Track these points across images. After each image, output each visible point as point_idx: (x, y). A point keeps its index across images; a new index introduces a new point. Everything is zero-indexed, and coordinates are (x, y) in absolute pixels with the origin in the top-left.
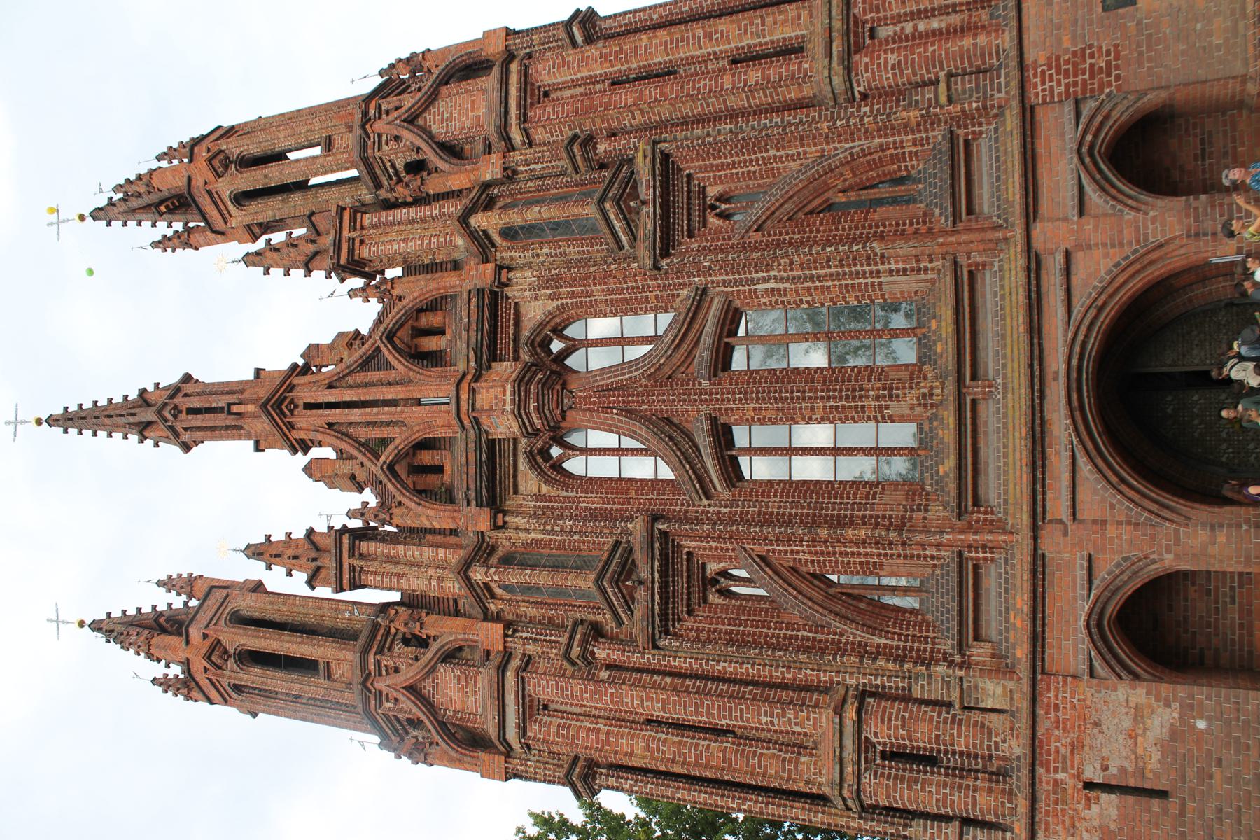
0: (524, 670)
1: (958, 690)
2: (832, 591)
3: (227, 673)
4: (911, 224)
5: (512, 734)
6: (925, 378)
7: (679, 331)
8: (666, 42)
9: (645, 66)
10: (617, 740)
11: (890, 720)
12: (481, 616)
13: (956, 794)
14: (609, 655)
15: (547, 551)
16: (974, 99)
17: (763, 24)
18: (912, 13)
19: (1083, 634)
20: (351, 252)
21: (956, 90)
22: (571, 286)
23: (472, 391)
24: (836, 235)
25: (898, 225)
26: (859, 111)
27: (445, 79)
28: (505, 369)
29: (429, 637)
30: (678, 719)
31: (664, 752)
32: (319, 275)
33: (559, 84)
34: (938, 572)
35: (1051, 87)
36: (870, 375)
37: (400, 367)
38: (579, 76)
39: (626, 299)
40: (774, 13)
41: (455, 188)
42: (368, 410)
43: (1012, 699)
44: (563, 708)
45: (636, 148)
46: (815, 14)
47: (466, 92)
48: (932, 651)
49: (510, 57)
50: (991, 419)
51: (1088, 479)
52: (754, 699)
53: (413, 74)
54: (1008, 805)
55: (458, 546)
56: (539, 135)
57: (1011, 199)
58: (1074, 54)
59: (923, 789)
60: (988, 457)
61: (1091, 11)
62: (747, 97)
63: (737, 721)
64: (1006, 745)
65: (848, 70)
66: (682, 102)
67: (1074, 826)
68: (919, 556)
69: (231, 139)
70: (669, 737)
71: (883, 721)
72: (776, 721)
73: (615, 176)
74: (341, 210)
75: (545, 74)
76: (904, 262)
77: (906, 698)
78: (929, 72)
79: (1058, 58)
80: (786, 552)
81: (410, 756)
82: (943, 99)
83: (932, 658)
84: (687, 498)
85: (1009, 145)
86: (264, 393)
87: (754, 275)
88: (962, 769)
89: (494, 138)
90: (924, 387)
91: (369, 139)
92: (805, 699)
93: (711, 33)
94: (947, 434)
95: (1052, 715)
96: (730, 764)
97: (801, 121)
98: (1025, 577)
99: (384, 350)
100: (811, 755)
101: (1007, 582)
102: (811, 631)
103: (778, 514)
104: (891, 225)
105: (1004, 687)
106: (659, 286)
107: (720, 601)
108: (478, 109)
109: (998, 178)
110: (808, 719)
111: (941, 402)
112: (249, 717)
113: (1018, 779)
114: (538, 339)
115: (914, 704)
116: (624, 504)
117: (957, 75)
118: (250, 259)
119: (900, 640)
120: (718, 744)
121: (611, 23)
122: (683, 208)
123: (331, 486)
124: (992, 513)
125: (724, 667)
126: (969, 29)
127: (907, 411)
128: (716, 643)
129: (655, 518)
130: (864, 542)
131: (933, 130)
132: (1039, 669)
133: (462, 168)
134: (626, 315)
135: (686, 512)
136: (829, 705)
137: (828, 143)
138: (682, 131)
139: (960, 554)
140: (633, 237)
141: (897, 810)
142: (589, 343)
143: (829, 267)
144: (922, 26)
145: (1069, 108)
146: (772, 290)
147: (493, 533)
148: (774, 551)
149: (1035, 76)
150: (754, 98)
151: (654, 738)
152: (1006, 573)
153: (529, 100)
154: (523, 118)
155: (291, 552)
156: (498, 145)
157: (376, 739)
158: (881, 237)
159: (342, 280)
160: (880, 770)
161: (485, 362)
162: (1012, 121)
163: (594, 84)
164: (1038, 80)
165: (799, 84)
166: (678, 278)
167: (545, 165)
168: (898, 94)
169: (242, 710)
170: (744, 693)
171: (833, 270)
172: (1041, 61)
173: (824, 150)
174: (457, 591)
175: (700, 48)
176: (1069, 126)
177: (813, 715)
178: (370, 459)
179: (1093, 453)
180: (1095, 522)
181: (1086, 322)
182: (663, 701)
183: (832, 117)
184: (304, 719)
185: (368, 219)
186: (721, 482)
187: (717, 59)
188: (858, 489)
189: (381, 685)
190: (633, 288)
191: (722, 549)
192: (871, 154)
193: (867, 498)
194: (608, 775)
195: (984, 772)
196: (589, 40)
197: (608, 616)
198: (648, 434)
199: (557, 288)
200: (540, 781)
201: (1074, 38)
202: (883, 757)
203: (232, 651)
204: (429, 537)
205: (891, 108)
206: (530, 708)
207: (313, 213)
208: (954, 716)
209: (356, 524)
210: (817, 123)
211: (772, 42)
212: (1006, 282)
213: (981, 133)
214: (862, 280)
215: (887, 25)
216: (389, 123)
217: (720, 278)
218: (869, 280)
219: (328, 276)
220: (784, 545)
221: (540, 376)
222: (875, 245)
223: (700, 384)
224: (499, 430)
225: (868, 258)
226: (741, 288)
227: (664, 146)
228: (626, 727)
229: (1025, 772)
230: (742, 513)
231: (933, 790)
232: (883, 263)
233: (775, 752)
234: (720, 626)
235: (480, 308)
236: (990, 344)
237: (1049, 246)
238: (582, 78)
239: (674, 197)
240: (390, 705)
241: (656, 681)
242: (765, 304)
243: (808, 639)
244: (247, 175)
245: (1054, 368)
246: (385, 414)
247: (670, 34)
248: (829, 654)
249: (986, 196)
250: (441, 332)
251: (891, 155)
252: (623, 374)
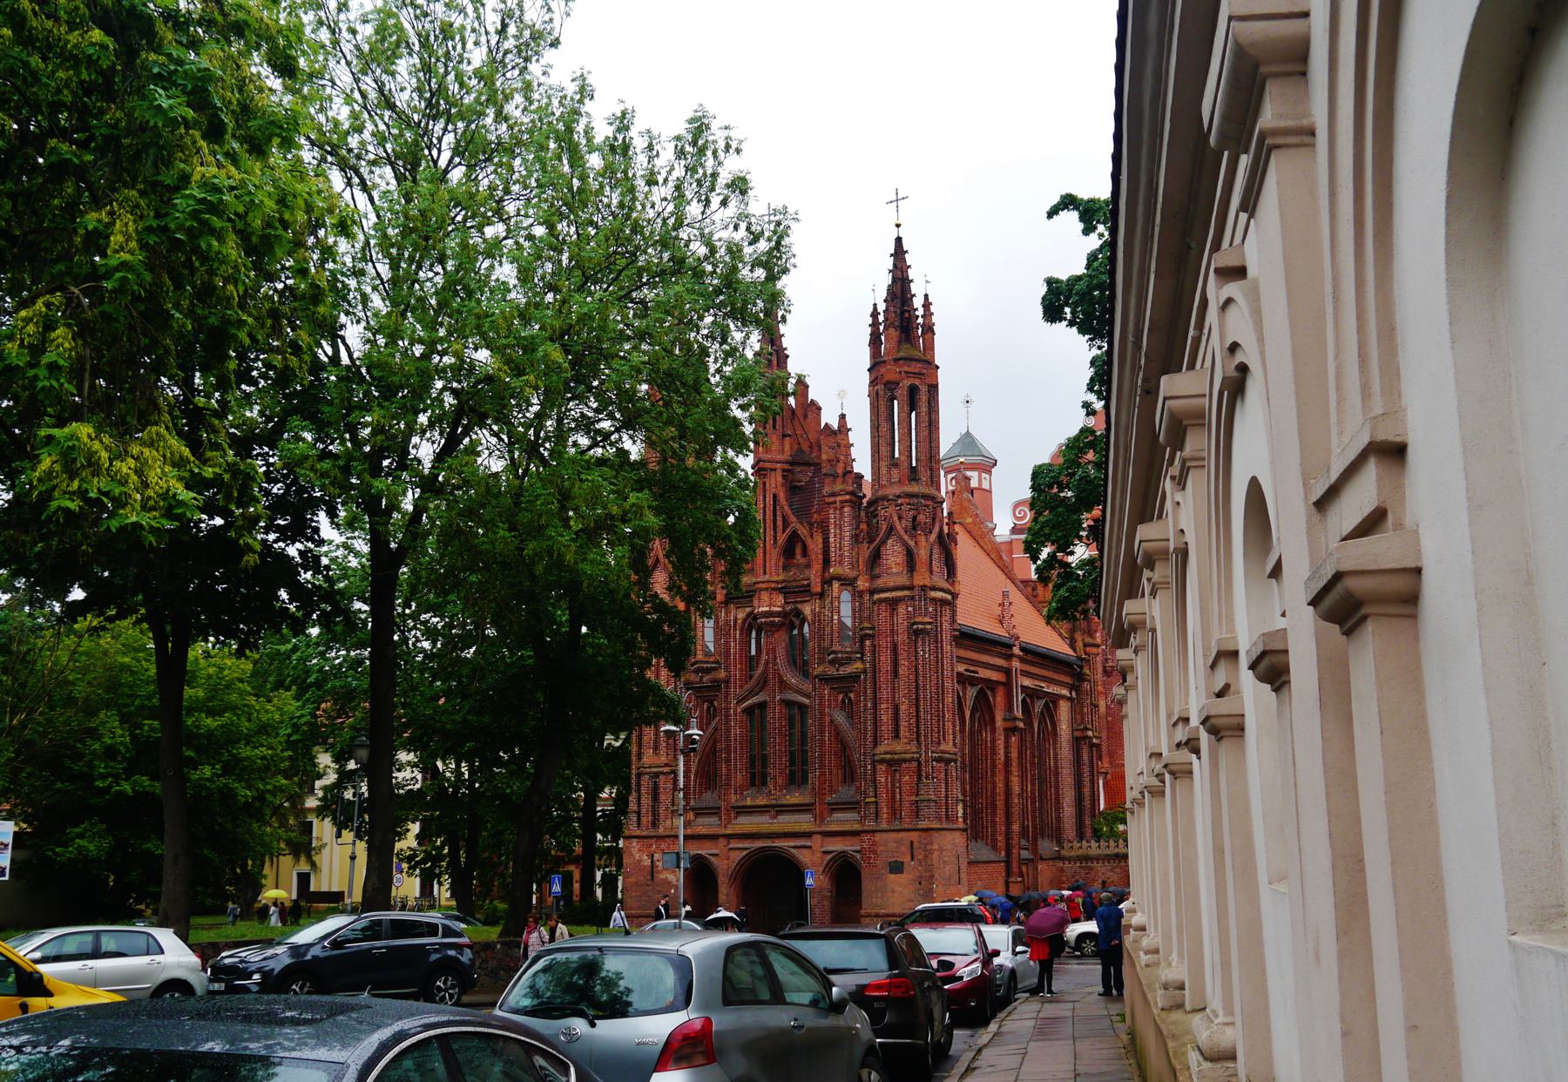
65: (882, 761)
75: (901, 609)
129: (727, 682)
154: (881, 601)
162: (857, 827)
235: (804, 586)
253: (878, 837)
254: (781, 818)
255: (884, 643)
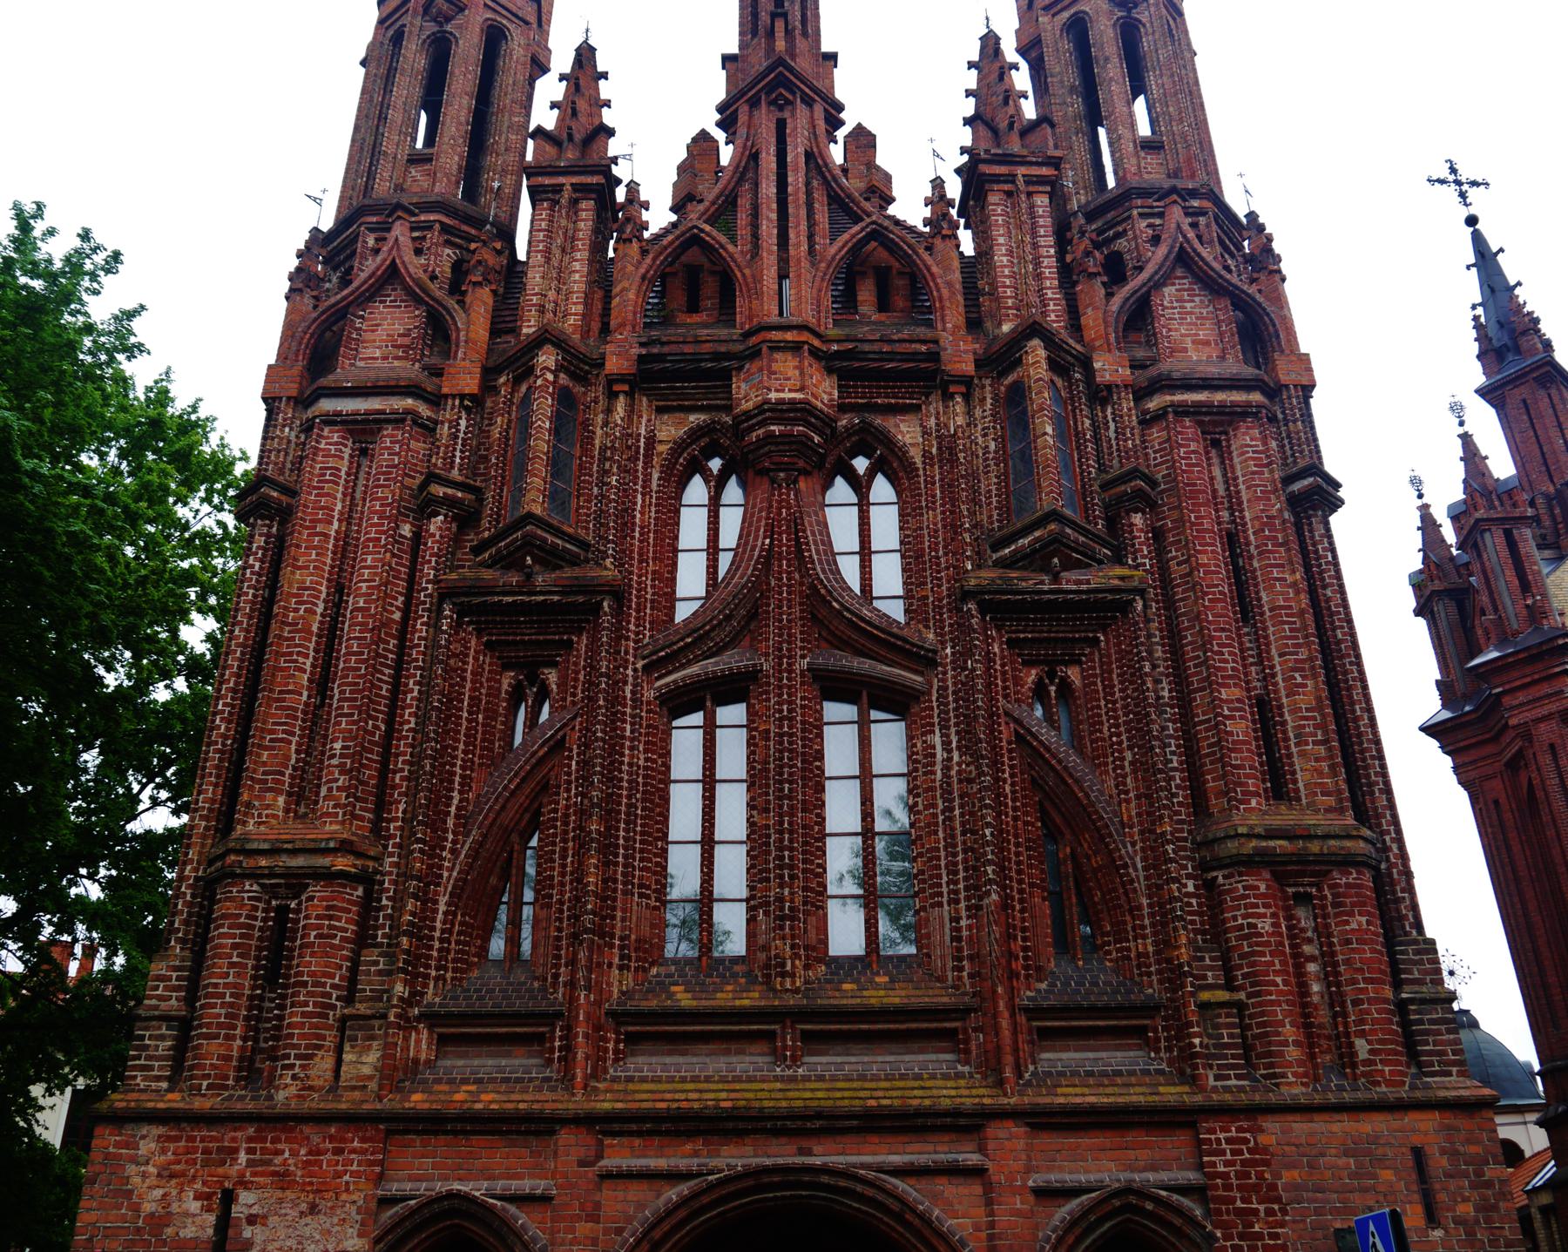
0: (415, 422)
1: (369, 1012)
2: (515, 838)
3: (418, 21)
4: (1025, 949)
5: (327, 405)
6: (807, 967)
7: (876, 628)
8: (1290, 607)
9: (1255, 578)
10: (315, 548)
11: (330, 918)
12: (491, 364)
13: (223, 1011)
14: (433, 535)
15: (577, 451)
16: (1206, 1040)
17: (1314, 743)
18: (1333, 954)
19: (440, 1187)
20: (997, 179)
21: (1219, 1016)
22: (941, 480)
23: (796, 348)
24: (1009, 842)
25: (1024, 930)
26: (1189, 876)
27: (1241, 302)
28: (825, 391)
29: (464, 293)
30: (342, 630)
31: (296, 610)
32: (966, 137)
33: (1231, 459)
34: (536, 984)
35: (1223, 1153)
36: (812, 890)
37: (833, 250)
38: (1242, 487)
39: (923, 556)
40: (1331, 757)
41: (1083, 321)
42: (774, 206)
43: (354, 1088)
44: (362, 475)
45: (1136, 567)
46: (1330, 816)
47: (1221, 334)
48: (427, 976)
49: (1274, 391)
50: (748, 1059)
51: (658, 1197)
52: (366, 731)
53: (1249, 259)
54: (205, 1083)
55: (585, 334)
56: (1156, 434)
57: (1059, 1090)
58: (1273, 1187)
59: (232, 965)
60: (695, 1055)
61: (1335, 1212)
62: (1208, 721)
63: (339, 708)
64: (289, 1081)
65: (1248, 863)
66: (1202, 629)
67: (171, 1176)
68: (558, 957)
69: (1164, 11)
70: (318, 618)
71: (328, 908)
72: (335, 762)
73: (1096, 538)
74: (1056, 163)
75: (1247, 441)
76: (970, 937)
77: (363, 940)
78: (1245, 976)
79: (1267, 1163)
80: (569, 774)
81: (299, 270)
82: (1205, 996)
83: (416, 975)
84: (646, 641)
85: (1138, 1090)
86: (803, 64)
87: (953, 730)
88: (258, 1019)
89: (1152, 372)
90: (793, 965)
91: (1158, 200)
92: (366, 801)
93: (1303, 670)
94: (726, 998)
95: (328, 1145)
96: (278, 700)
97: (1175, 795)
98: (521, 1106)
99: (857, 228)
100: (287, 811)
101: (518, 1080)
102: (458, 808)
103: (622, 763)
104: (1023, 920)
105: (370, 1078)
106: (940, 600)
107: (505, 687)
108: (1197, 350)
109: (1090, 1074)
110: (335, 806)
111: (775, 991)
112: (362, 54)
113: (242, 1098)
114: (869, 438)
115: (352, 951)
116: (640, 555)
117: (1241, 1017)
118: (990, 43)
119: (443, 931)
120: (305, 683)
121: (1319, 531)
122: (1049, 632)
123: (682, 169)
124: (616, 1060)
125: (412, 691)
126: (1309, 1036)
127: (761, 940)
128: (445, 680)
130: (579, 881)
131: (1160, 982)
132: (393, 1126)
133: (1111, 330)
134: (903, 557)
135: (627, 639)
136: (354, 834)
137: (1142, 832)
138: (1161, 630)
139: (558, 1015)
140: (1004, 564)
141: (207, 930)
142: (864, 506)
143: (964, 833)
144: (1312, 967)
145: (1192, 1176)
146: (934, 755)
147: (602, 379)
148: (571, 758)
149: (1239, 1130)
150: (1207, 730)
151: (318, 598)
152: (531, 1080)
153: (1207, 419)
154: (1182, 411)
155: (582, 105)
156: (1143, 377)
157: (327, 225)
158: (1005, 904)
159: (958, 171)
160: (261, 905)
161: (838, 364)
162: (1173, 1093)
163: (1231, 509)
164: (1234, 1134)
165: (1227, 793)
166: (951, 625)
167: (1114, 442)
168: (1215, 932)
169: (371, 48)
170: (376, 719)
171: (959, 839)
172: (1261, 1139)
173: (1131, 827)
174: (525, 331)
175: (1280, 655)
176: (1164, 1176)
177: (341, 812)
178: (707, 210)
179: (696, 1204)
180: (598, 1206)
181: (880, 1197)
182: (368, 609)
183: (1179, 839)
184: (357, 128)
185: (1042, 201)
186: (667, 685)
187: (1265, 679)
188: (655, 873)
189: (400, 231)
190: (938, 565)
191: (575, 687)
192: (1126, 893)
193: (641, 886)
194: (268, 535)
195: (253, 1050)
196: (1294, 502)
197: (486, 534)
198: (736, 585)
199: (940, 461)
200: (263, 445)
201: (1292, 1187)
202: (278, 909)
203: (448, 28)
204: (599, 294)
205: (1193, 922)
206: (362, 431)
207: (1053, 125)
208: (334, 1007)
209: (620, 194)
210: (1170, 817)
211: (1290, 756)
212: (940, 1083)
213: (1157, 1051)
214: (945, 879)
215: (1315, 918)
216: (1179, 227)
217: (950, 683)
218: (945, 890)
219: (963, 150)
220: (577, 771)
221: (817, 439)
222: (994, 897)
223: (803, 657)
224: (743, 386)
225: (977, 888)
226: (936, 711)
227: (1139, 606)
228: (333, 560)
229: (250, 1106)
230: (624, 713)
231: (231, 979)
232: (968, 908)
233: (293, 761)
234: (468, 685)
235: (913, 356)
236: (853, 1059)
237: (991, 1145)
238: (1238, 492)
239: (1066, 620)
240: (371, 242)
241: (396, 599)
242: (914, 745)
243: (449, 805)
244: (1110, 33)
245: (817, 1149)
246: (769, 230)
247: (1302, 613)
248: (425, 834)
249: (1064, 1055)
250: (883, 305)
251: (1125, 923)
252: (818, 552)
253: (1272, 1131)
254: (820, 1061)
255: (1207, 521)
